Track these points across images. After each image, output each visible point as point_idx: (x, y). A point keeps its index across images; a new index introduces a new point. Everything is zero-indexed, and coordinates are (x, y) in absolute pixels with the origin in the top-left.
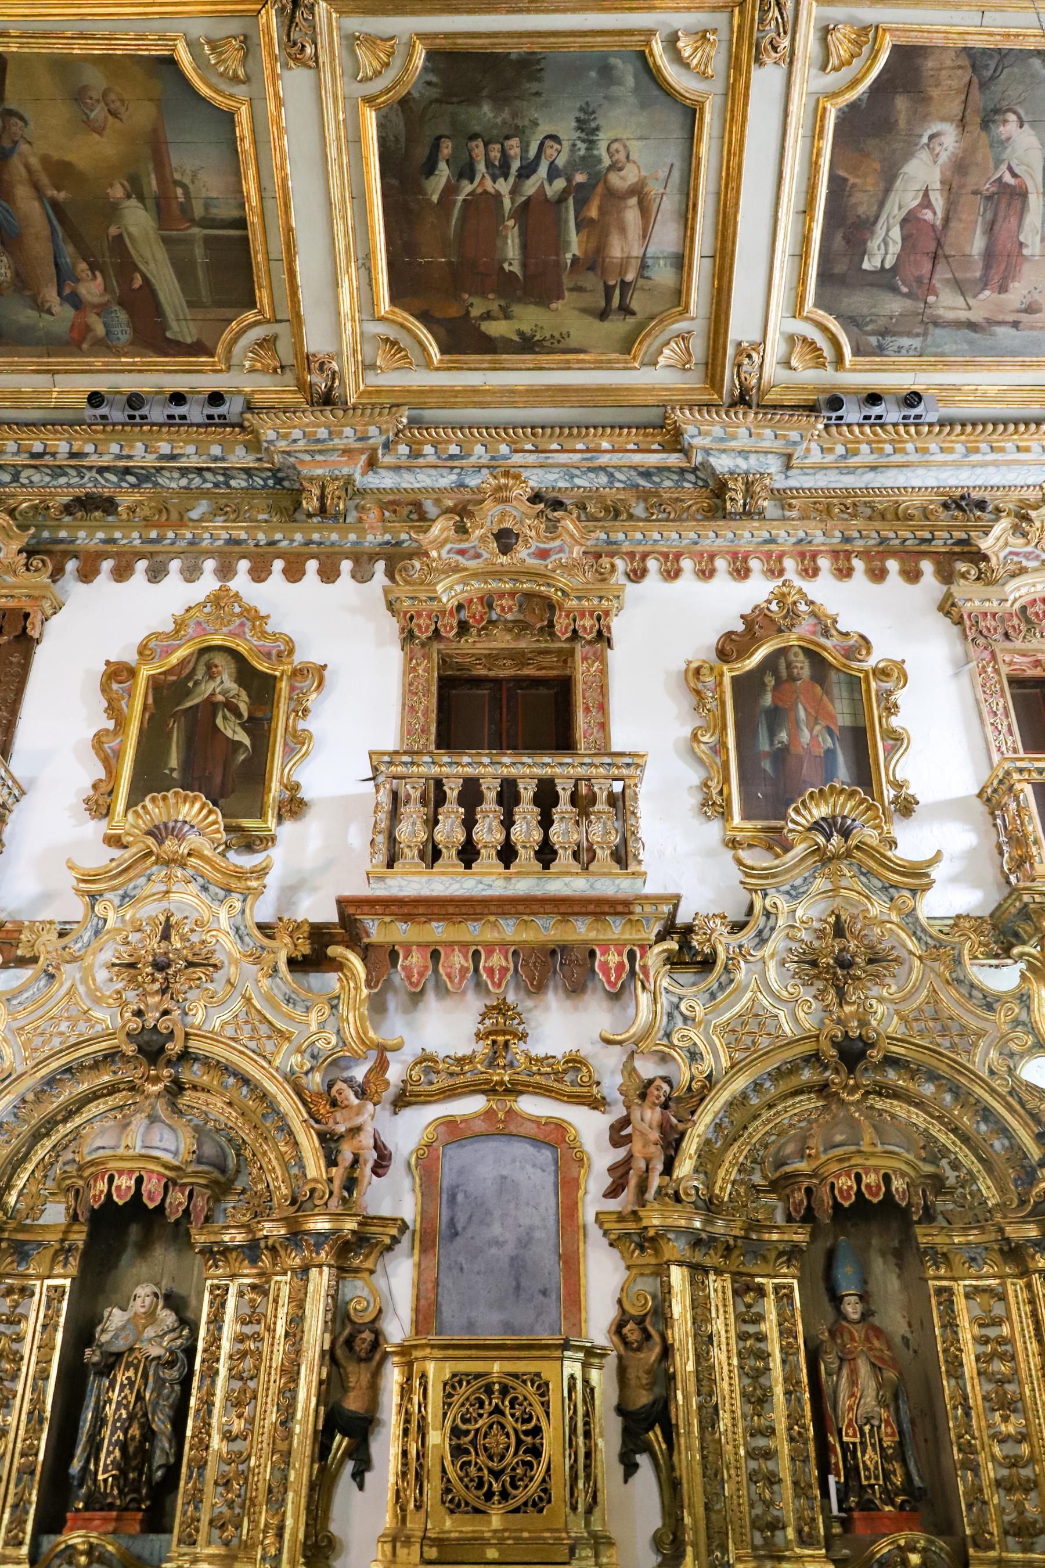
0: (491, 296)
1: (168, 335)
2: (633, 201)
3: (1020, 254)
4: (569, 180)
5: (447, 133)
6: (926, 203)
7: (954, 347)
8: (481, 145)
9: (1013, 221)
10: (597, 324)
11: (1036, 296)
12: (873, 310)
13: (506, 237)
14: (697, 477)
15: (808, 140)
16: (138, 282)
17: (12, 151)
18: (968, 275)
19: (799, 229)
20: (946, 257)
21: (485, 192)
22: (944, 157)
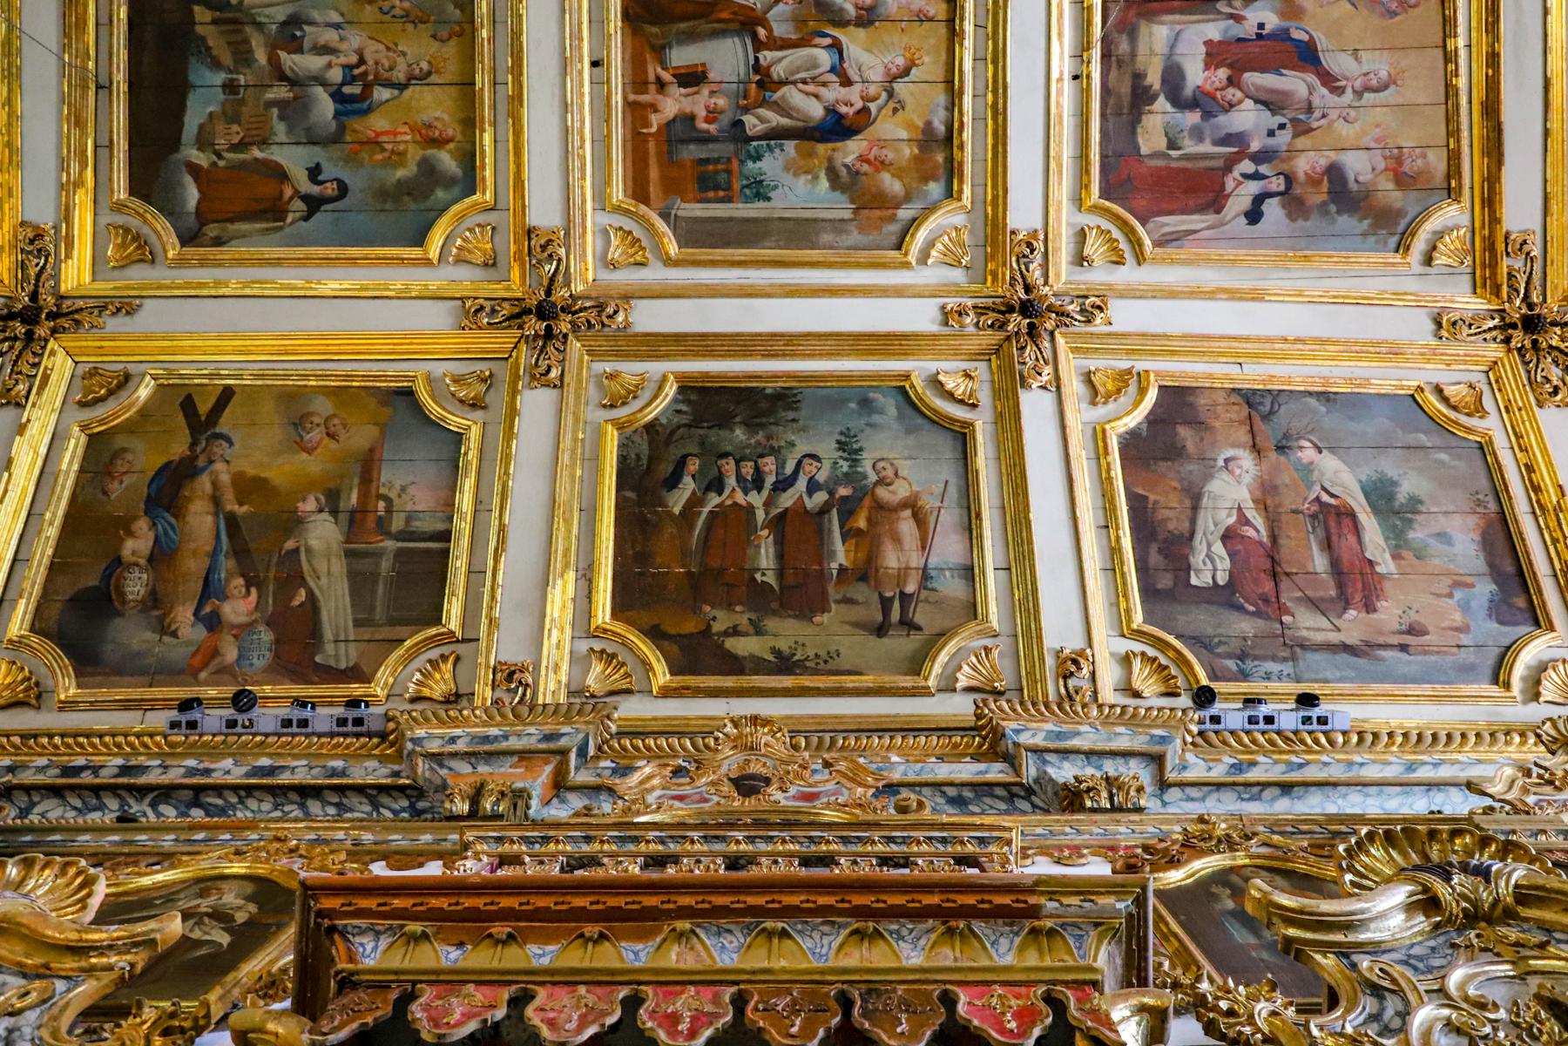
0: (738, 608)
1: (318, 659)
2: (908, 513)
3: (1374, 572)
4: (831, 493)
5: (695, 452)
6: (1243, 520)
7: (1338, 674)
8: (732, 462)
9: (1351, 539)
10: (873, 640)
11: (1414, 616)
12: (1219, 631)
13: (759, 546)
14: (1034, 806)
15: (1093, 462)
16: (301, 596)
17: (203, 469)
18: (1321, 593)
19: (1105, 542)
20: (1287, 574)
21: (735, 504)
22: (1247, 479)
